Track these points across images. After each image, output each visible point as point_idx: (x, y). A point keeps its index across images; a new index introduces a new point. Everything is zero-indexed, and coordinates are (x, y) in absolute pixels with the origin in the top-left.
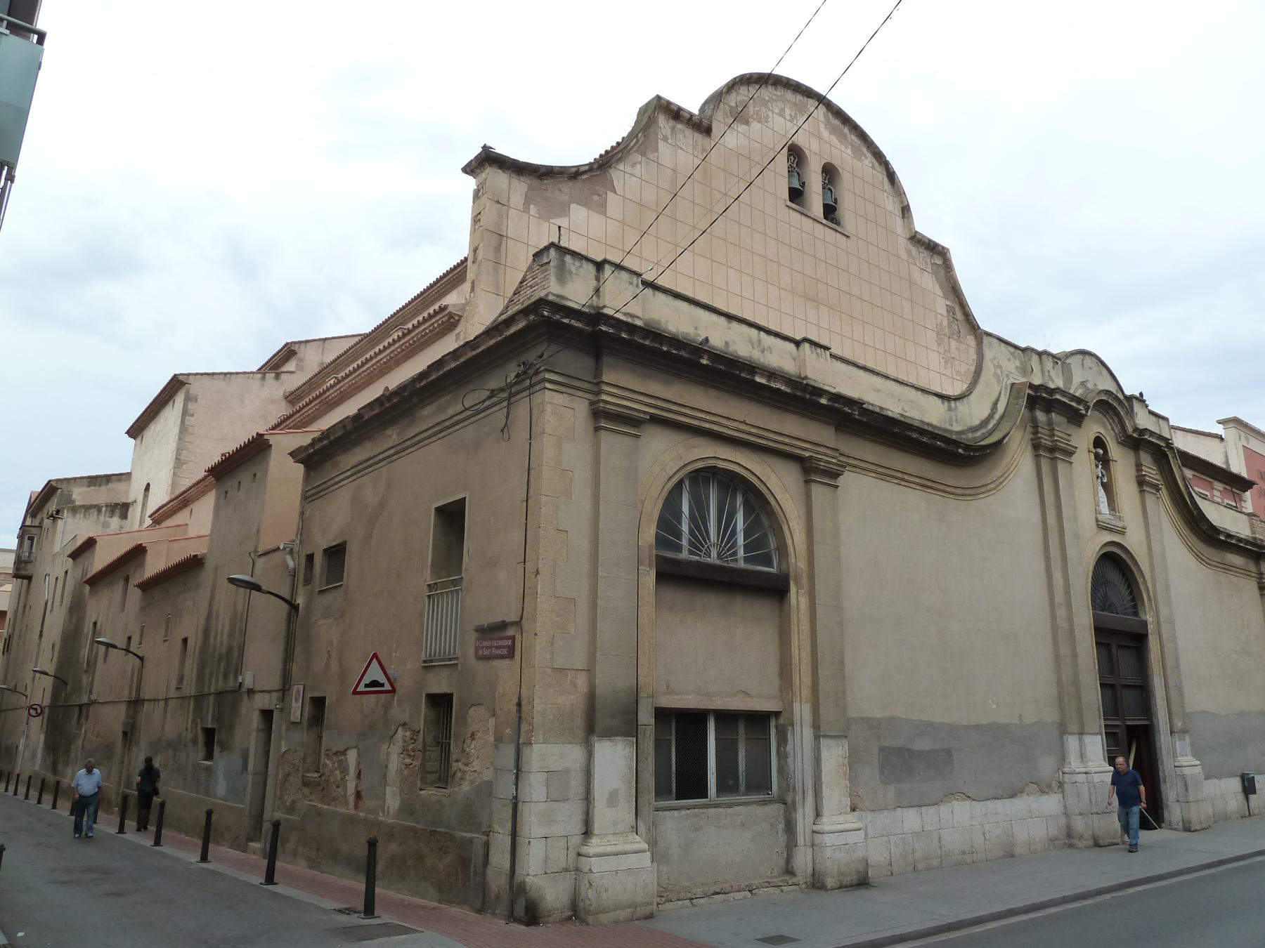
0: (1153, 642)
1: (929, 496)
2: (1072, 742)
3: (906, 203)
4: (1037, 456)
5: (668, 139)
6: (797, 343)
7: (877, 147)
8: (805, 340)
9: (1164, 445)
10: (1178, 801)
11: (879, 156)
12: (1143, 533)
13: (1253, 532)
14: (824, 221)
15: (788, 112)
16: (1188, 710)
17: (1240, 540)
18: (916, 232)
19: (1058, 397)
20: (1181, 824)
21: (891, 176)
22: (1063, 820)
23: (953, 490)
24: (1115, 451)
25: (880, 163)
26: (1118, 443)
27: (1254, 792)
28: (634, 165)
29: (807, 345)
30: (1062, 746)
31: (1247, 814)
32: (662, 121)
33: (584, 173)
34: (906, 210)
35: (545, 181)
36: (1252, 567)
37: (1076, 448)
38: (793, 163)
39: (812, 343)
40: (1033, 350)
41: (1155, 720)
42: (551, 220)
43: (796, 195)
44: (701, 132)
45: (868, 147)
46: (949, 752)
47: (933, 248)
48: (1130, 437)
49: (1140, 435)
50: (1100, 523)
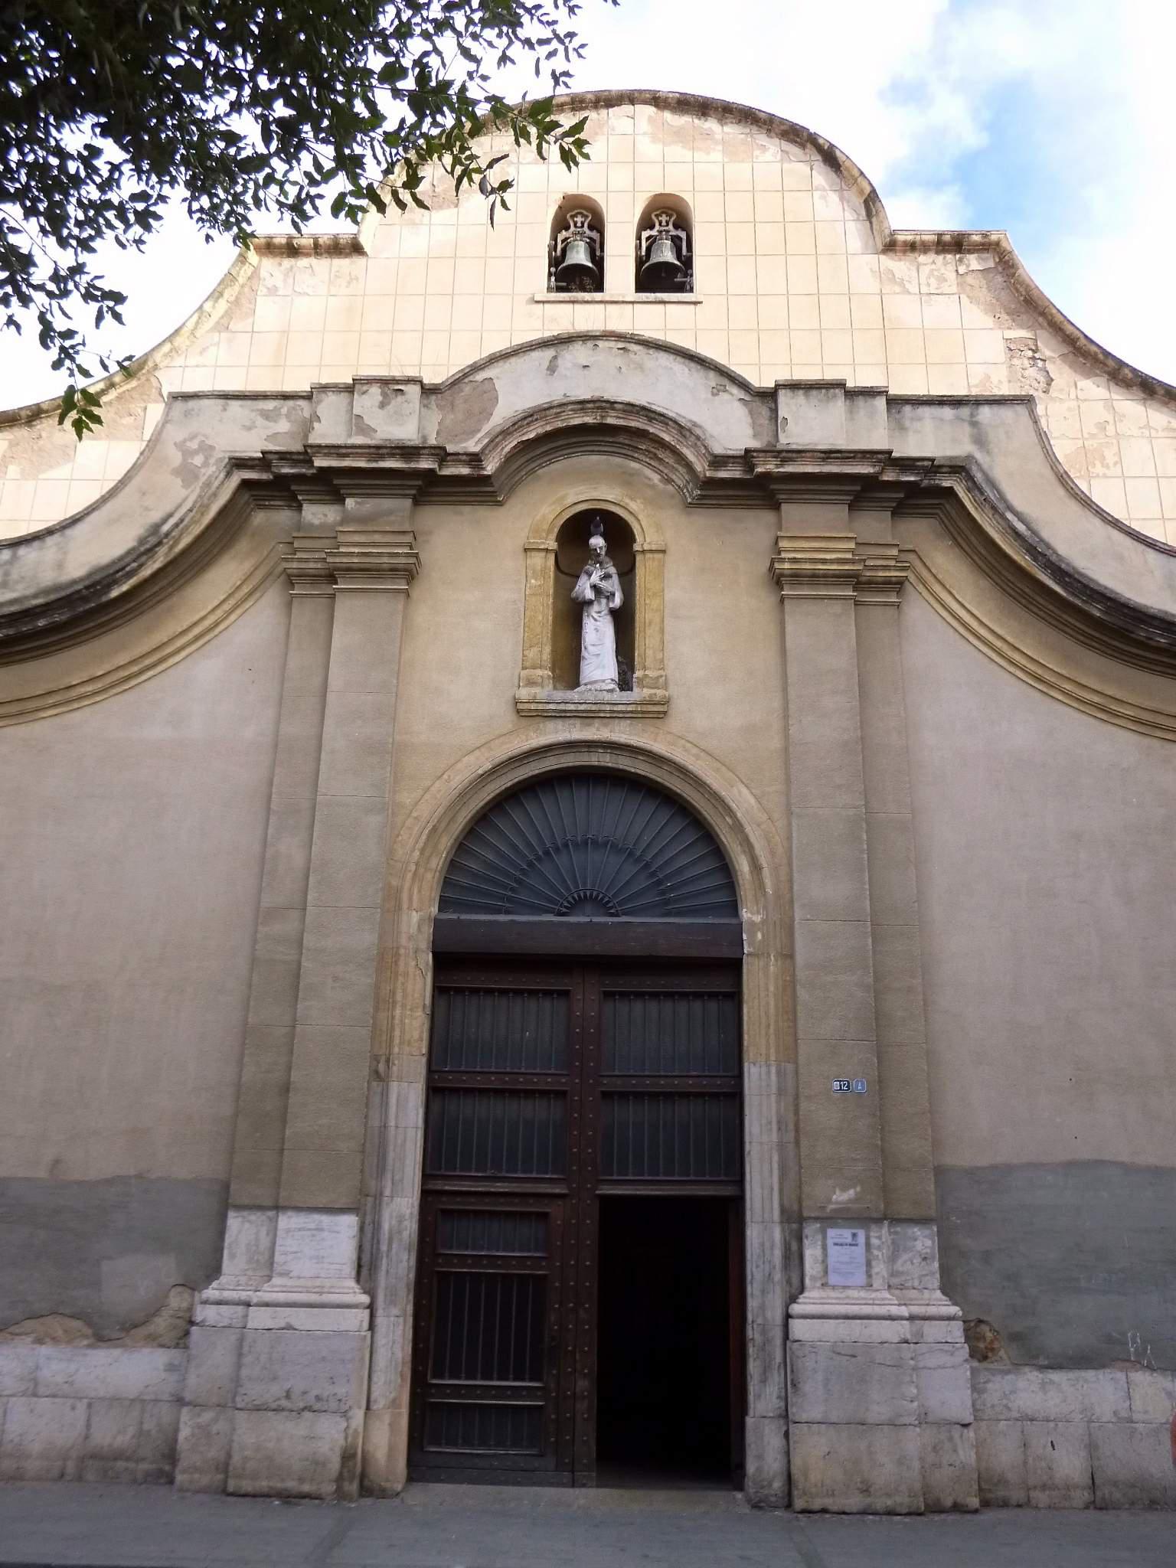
2: (241, 1229)
3: (868, 190)
7: (782, 121)
14: (644, 296)
18: (893, 233)
19: (319, 462)
25: (803, 146)
30: (221, 1233)
35: (38, 427)
38: (583, 226)
40: (324, 388)
44: (347, 255)
45: (769, 131)
48: (710, 483)
50: (520, 706)
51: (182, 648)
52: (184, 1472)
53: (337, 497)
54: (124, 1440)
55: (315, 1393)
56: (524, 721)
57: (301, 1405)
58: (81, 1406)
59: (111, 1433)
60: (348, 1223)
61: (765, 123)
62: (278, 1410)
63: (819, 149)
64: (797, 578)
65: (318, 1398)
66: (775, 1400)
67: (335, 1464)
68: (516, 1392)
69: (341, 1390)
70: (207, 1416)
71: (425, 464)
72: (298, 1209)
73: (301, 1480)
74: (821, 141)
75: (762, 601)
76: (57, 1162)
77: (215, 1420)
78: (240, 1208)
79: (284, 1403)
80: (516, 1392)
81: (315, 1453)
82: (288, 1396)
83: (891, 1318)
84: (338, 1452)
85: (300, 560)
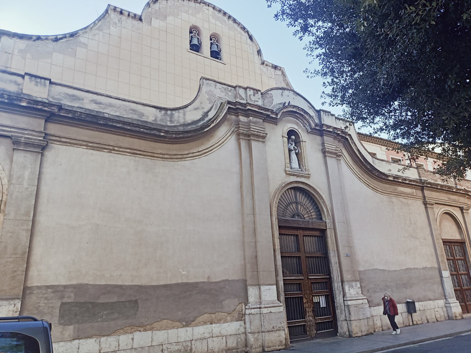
0: (330, 234)
1: (137, 159)
3: (259, 49)
4: (238, 139)
5: (117, 24)
6: (23, 77)
7: (242, 25)
8: (26, 74)
9: (340, 133)
10: (346, 320)
11: (244, 28)
12: (238, 166)
13: (420, 176)
14: (211, 58)
15: (190, 12)
16: (361, 269)
17: (411, 181)
19: (248, 107)
20: (347, 333)
21: (251, 38)
22: (243, 337)
23: (161, 156)
24: (304, 136)
26: (308, 132)
27: (415, 311)
28: (94, 35)
29: (27, 77)
30: (247, 293)
31: (411, 324)
32: (113, 16)
33: (61, 39)
34: (259, 52)
36: (419, 193)
37: (267, 134)
38: (196, 34)
39: (31, 76)
40: (240, 87)
41: (332, 275)
42: (40, 60)
43: (196, 48)
46: (136, 301)
47: (275, 67)
49: (321, 128)
50: (287, 172)
51: (217, 147)
52: (254, 349)
53: (248, 116)
54: (234, 345)
55: (278, 326)
56: (287, 176)
57: (276, 329)
58: (224, 338)
59: (232, 343)
60: (275, 287)
61: (238, 23)
62: (272, 331)
63: (249, 34)
64: (328, 152)
65: (279, 327)
66: (344, 317)
67: (284, 342)
68: (299, 322)
69: (283, 325)
70: (256, 335)
71: (269, 113)
72: (265, 285)
73: (279, 346)
74: (249, 33)
75: (320, 155)
76: (209, 277)
77: (258, 336)
78: (252, 285)
79: (273, 330)
80: (299, 322)
81: (280, 339)
82: (273, 328)
83: (360, 299)
84: (284, 338)
85: (243, 130)
